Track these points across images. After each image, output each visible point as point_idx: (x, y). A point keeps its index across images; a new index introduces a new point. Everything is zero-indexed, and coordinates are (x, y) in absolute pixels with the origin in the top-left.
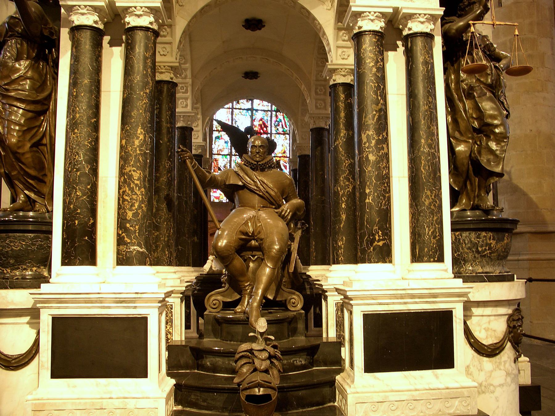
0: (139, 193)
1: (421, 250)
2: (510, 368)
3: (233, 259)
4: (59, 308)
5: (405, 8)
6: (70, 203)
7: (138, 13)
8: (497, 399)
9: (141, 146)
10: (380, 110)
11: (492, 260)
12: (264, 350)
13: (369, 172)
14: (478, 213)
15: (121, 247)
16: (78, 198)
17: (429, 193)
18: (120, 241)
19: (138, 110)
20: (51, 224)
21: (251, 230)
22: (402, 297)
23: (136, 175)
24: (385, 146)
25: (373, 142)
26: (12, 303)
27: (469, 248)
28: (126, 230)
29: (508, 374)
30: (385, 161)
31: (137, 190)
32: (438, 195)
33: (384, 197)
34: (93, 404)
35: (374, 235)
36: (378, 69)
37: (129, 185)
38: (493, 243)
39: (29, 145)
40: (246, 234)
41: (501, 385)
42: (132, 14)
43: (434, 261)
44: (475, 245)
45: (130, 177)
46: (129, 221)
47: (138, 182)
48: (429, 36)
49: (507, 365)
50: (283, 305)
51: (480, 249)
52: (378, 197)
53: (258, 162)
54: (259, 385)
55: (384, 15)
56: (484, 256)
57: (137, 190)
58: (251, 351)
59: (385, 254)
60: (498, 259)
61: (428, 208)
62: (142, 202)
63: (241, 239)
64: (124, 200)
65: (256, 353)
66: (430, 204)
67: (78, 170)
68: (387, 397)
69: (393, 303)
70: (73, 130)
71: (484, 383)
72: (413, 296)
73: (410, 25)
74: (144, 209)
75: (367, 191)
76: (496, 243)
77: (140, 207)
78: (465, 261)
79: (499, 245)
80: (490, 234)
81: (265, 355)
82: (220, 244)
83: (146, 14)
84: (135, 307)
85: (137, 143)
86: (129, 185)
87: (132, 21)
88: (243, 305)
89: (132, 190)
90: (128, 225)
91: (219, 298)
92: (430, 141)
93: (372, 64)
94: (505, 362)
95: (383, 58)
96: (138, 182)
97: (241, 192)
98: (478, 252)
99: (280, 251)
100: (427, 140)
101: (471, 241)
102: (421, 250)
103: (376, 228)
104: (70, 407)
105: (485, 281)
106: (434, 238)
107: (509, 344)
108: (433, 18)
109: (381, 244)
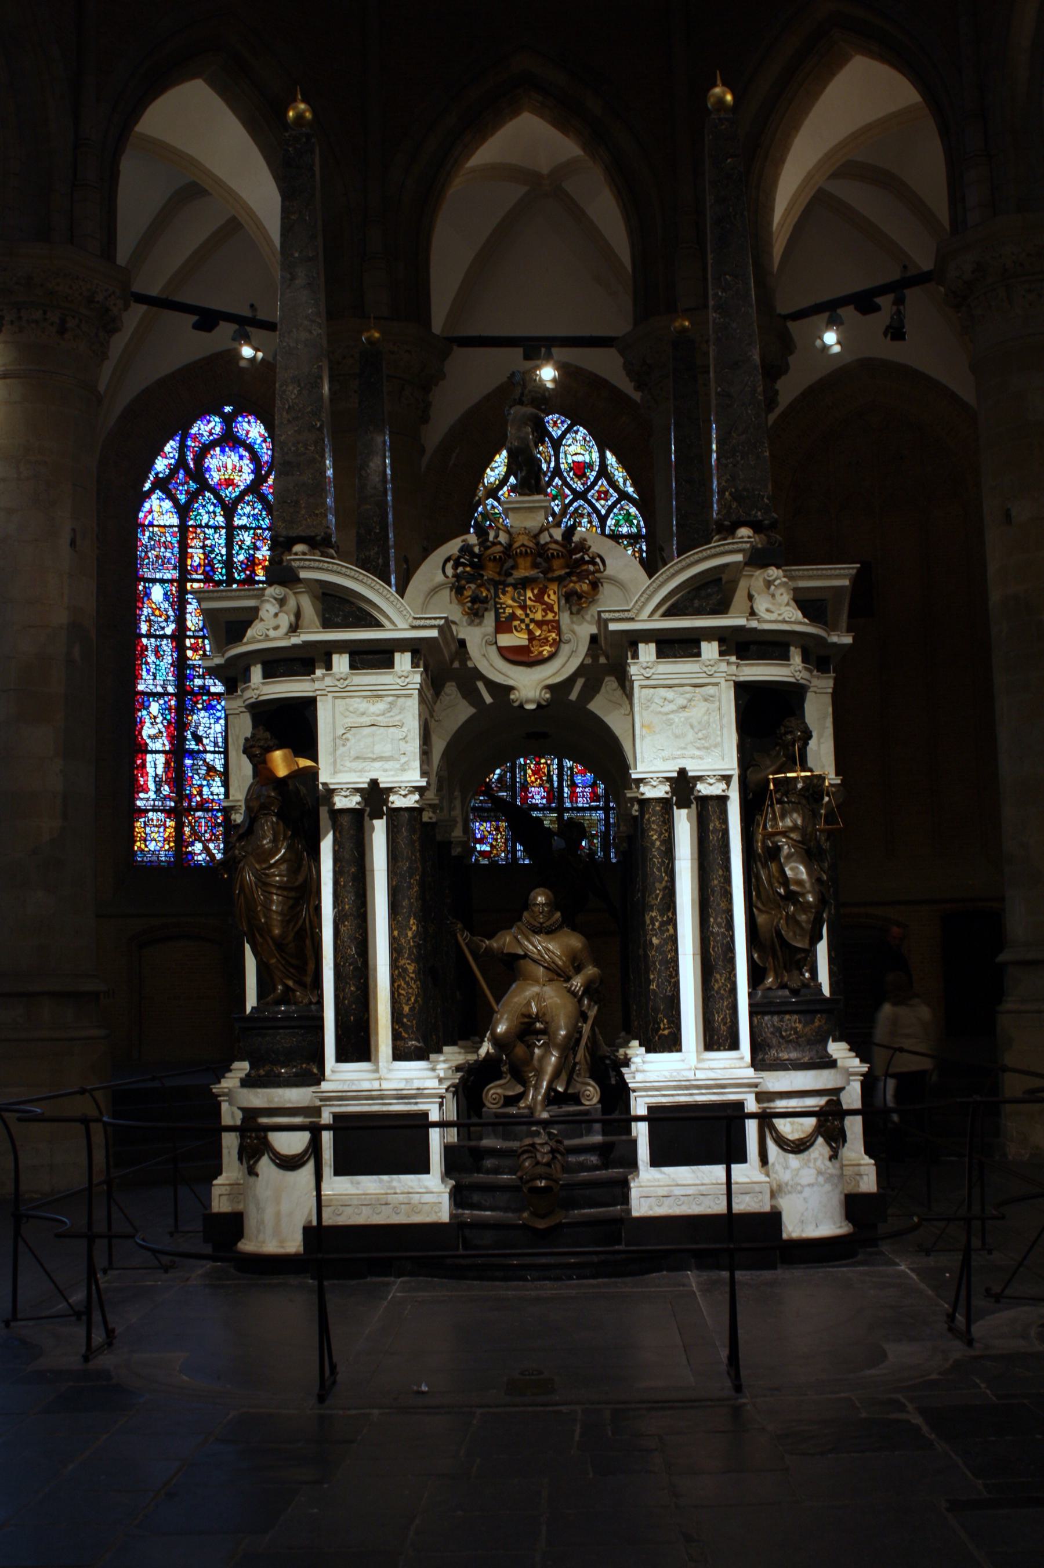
0: (414, 986)
1: (711, 1037)
2: (823, 1167)
3: (515, 1046)
4: (340, 1105)
6: (344, 998)
7: (403, 793)
8: (805, 1200)
9: (414, 937)
10: (666, 888)
11: (800, 1046)
12: (546, 1143)
13: (653, 956)
14: (787, 992)
15: (399, 1043)
16: (352, 993)
17: (718, 976)
18: (396, 1036)
19: (409, 899)
20: (321, 1019)
21: (535, 1010)
22: (687, 1088)
23: (411, 968)
24: (670, 928)
25: (657, 924)
26: (290, 1101)
27: (772, 1033)
28: (403, 1025)
29: (820, 1173)
30: (670, 943)
31: (412, 984)
32: (729, 978)
33: (670, 982)
34: (378, 1199)
35: (659, 1024)
36: (663, 842)
37: (404, 979)
38: (799, 1026)
39: (292, 935)
40: (529, 1016)
41: (810, 1185)
42: (396, 793)
43: (725, 1050)
44: (779, 1030)
45: (405, 970)
46: (406, 1016)
47: (413, 975)
48: (723, 800)
49: (819, 1163)
50: (576, 1099)
51: (784, 1034)
52: (663, 983)
53: (541, 924)
54: (541, 1177)
55: (668, 779)
56: (790, 1041)
57: (412, 984)
58: (533, 1145)
59: (673, 1043)
60: (808, 1044)
61: (717, 993)
62: (417, 996)
63: (522, 1023)
64: (399, 994)
65: (538, 1147)
66: (719, 988)
67: (350, 965)
68: (671, 1191)
69: (678, 1095)
70: (343, 923)
71: (790, 1183)
72: (698, 1087)
73: (700, 786)
74: (421, 1002)
75: (652, 977)
76: (804, 1026)
77: (416, 1001)
78: (770, 1047)
79: (807, 1029)
80: (795, 1017)
81: (546, 1149)
82: (499, 1030)
83: (411, 792)
84: (416, 1103)
85: (410, 934)
86: (404, 979)
87: (397, 801)
88: (527, 1099)
89: (408, 984)
90: (405, 1020)
91: (499, 1091)
92: (719, 920)
93: (655, 837)
94: (815, 1159)
95: (669, 828)
96: (413, 975)
97: (522, 961)
98: (782, 1037)
99: (568, 1037)
100: (715, 919)
101: (773, 1026)
102: (711, 1037)
103: (660, 1016)
104: (355, 1202)
105: (788, 1069)
106: (725, 1024)
107: (820, 1140)
108: (727, 779)
109: (666, 1032)
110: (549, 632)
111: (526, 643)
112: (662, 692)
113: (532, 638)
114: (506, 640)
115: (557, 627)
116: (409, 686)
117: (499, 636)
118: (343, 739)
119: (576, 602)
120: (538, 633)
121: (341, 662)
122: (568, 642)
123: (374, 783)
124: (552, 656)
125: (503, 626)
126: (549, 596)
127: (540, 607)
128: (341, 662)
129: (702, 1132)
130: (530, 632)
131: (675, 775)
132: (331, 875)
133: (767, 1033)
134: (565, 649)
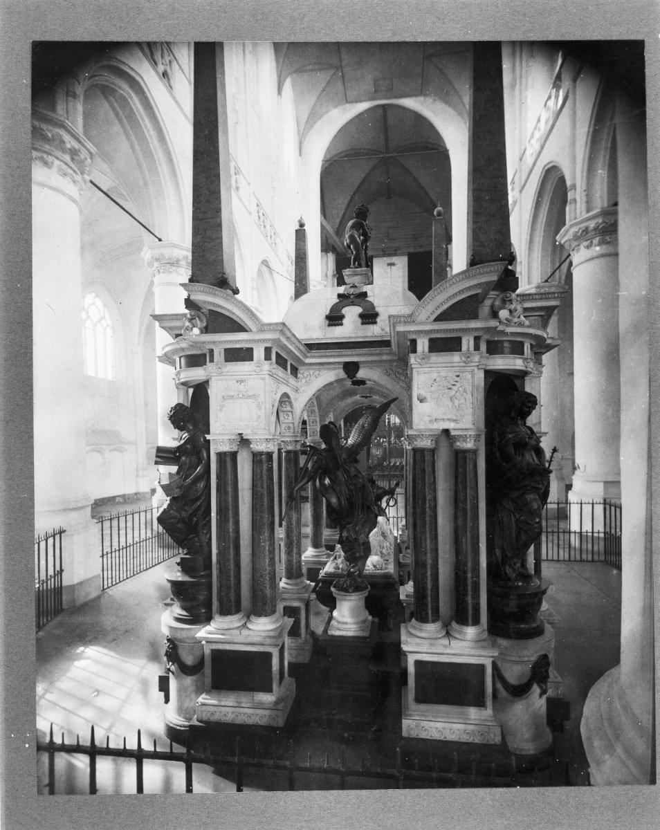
121: (219, 355)
129: (449, 685)
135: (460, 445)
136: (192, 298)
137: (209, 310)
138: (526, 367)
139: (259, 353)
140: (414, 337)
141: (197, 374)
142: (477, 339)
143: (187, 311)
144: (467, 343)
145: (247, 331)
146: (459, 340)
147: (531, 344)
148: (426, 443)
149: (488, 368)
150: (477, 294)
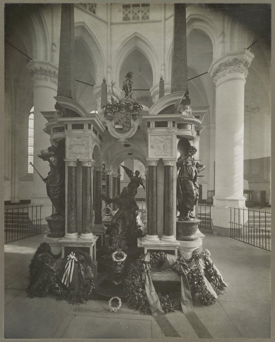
5: (165, 159)
72: (162, 246)
73: (166, 164)
110: (128, 125)
111: (122, 127)
112: (157, 137)
113: (123, 126)
114: (117, 127)
115: (130, 124)
116: (87, 134)
117: (115, 125)
118: (70, 148)
119: (134, 118)
120: (125, 124)
121: (70, 127)
122: (133, 127)
123: (78, 160)
124: (129, 130)
125: (117, 124)
126: (128, 116)
127: (126, 118)
128: (70, 127)
130: (123, 125)
131: (159, 160)
132: (67, 184)
133: (180, 231)
134: (132, 130)
135: (167, 164)
136: (59, 103)
137: (66, 109)
138: (192, 135)
139: (86, 127)
140: (149, 121)
141: (59, 135)
142: (174, 122)
143: (55, 110)
144: (170, 125)
145: (81, 117)
146: (166, 123)
147: (195, 126)
148: (154, 164)
149: (178, 134)
150: (174, 105)
